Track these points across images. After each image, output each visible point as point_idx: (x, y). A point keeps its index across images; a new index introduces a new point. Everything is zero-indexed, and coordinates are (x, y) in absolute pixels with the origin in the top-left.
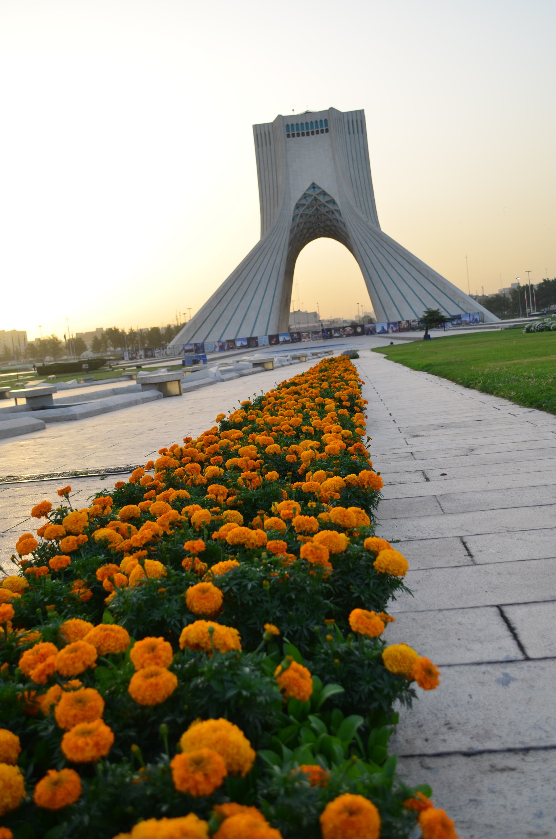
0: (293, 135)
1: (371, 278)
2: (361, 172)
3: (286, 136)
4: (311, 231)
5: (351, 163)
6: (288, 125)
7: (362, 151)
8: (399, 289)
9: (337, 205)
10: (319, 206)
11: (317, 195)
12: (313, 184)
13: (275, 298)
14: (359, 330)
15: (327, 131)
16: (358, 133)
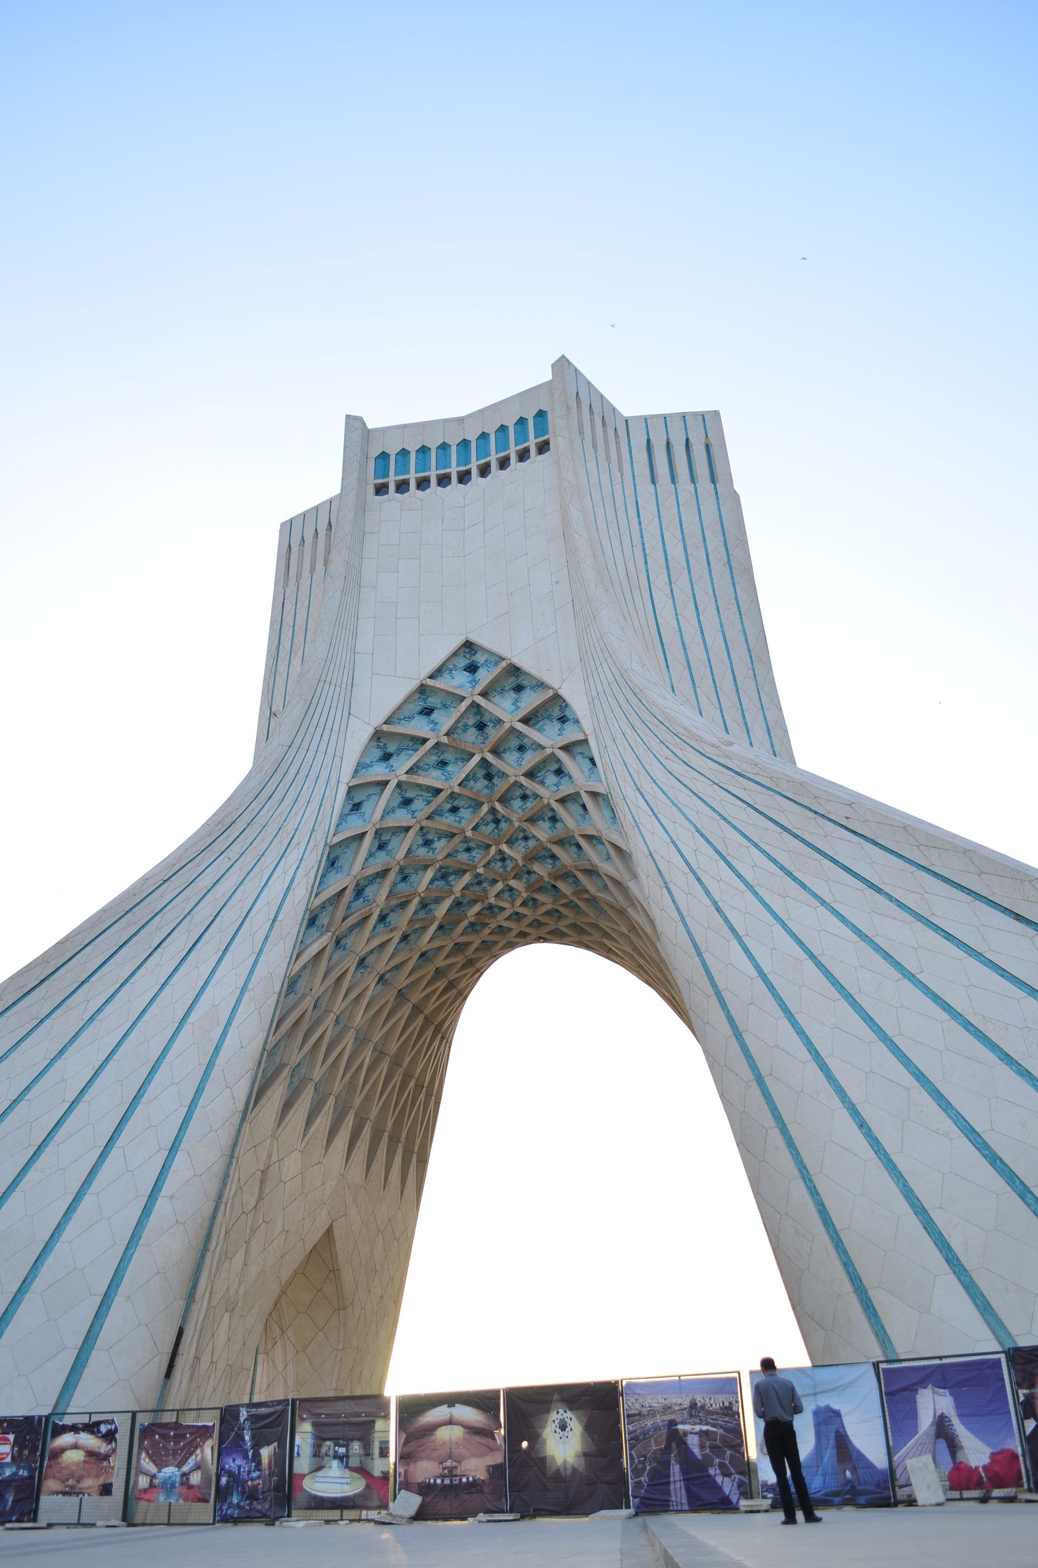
0: (402, 487)
1: (760, 1080)
2: (709, 614)
3: (371, 489)
4: (459, 884)
5: (660, 580)
6: (384, 456)
7: (714, 542)
8: (971, 1133)
9: (577, 722)
10: (495, 751)
11: (484, 694)
12: (469, 646)
13: (162, 1205)
14: (563, 1444)
15: (543, 448)
16: (693, 480)
